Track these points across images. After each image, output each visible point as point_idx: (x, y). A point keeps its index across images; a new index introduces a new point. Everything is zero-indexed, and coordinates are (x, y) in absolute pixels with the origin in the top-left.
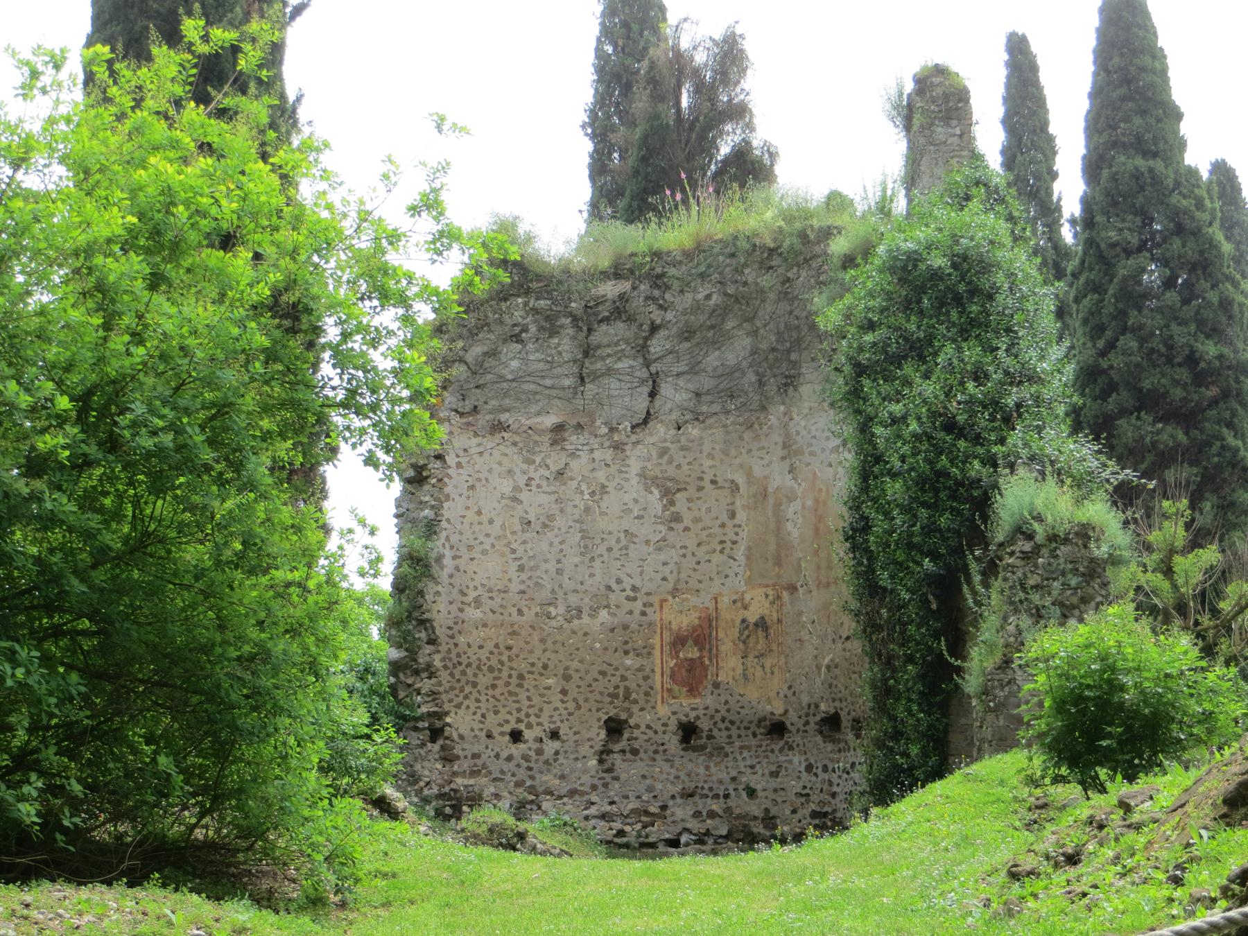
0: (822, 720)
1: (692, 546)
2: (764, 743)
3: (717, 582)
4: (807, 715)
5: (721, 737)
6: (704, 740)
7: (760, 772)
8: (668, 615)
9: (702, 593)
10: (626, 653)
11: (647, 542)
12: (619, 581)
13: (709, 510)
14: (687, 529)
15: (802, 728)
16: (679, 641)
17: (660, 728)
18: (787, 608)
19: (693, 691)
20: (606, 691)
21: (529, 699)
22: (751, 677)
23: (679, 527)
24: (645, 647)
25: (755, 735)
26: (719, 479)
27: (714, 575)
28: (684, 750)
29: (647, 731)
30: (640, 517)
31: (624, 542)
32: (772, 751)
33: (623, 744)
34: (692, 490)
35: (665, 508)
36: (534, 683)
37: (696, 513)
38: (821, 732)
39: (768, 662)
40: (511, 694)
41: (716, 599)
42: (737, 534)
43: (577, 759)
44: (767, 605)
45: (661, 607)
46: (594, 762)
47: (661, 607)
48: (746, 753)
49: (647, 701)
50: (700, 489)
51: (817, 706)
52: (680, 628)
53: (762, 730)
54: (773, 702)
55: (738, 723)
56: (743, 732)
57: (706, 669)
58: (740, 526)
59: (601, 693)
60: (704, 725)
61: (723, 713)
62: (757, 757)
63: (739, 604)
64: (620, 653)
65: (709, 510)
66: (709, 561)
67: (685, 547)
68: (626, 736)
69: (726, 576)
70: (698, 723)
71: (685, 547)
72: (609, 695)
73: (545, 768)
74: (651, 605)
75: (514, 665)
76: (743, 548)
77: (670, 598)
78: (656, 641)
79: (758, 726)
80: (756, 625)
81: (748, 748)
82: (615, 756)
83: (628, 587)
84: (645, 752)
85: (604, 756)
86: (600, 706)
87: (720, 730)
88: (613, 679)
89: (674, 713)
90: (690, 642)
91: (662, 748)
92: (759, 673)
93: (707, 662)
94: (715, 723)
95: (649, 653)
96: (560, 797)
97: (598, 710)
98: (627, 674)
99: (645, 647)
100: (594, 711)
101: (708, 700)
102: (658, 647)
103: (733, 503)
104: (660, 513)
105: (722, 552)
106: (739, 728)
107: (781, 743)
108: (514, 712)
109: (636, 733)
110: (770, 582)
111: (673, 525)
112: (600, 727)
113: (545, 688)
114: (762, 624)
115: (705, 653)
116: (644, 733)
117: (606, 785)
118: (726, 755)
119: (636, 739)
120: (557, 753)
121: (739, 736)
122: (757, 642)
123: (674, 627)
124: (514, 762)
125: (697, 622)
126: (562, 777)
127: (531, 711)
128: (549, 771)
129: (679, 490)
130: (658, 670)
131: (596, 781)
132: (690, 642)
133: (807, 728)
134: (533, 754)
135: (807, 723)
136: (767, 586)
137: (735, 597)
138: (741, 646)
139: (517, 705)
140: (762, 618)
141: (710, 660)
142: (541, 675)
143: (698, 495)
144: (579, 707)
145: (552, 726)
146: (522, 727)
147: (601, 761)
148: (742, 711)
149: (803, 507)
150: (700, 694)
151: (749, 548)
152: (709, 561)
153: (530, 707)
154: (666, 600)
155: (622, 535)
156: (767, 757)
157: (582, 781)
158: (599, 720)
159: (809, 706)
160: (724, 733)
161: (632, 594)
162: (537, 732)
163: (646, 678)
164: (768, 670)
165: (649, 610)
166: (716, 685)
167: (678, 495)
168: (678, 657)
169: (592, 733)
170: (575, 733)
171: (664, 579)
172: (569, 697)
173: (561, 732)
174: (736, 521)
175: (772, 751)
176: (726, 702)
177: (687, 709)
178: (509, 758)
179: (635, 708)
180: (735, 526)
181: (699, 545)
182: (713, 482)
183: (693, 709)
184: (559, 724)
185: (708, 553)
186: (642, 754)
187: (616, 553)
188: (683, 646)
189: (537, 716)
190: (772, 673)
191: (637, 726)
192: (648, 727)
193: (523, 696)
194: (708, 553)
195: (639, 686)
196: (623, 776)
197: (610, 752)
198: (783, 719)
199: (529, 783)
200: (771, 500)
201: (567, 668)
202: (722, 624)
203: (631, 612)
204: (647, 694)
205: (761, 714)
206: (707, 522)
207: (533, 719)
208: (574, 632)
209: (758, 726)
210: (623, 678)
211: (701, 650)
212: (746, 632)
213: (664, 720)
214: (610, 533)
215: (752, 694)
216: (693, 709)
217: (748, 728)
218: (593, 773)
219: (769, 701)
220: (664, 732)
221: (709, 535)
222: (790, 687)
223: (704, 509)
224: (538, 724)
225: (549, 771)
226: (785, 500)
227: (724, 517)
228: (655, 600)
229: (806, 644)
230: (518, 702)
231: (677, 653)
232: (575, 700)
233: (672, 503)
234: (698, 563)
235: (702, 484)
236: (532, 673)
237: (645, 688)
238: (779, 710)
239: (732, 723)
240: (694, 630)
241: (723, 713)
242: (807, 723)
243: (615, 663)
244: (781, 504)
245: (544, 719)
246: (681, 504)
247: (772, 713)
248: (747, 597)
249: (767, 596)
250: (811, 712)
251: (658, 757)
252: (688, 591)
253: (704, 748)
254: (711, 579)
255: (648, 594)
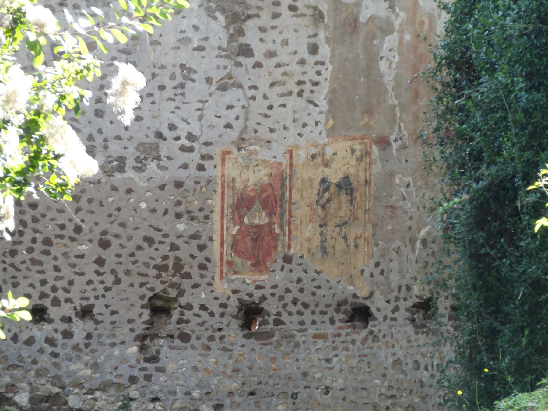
0: (414, 306)
1: (264, 87)
2: (344, 332)
3: (293, 131)
4: (397, 299)
5: (291, 322)
6: (271, 326)
7: (337, 367)
8: (232, 170)
9: (274, 145)
10: (178, 216)
11: (209, 80)
12: (172, 127)
13: (285, 43)
14: (258, 65)
15: (390, 315)
16: (243, 204)
17: (217, 310)
18: (377, 167)
19: (258, 265)
20: (153, 263)
21: (57, 269)
22: (330, 250)
23: (248, 62)
24: (201, 210)
25: (332, 322)
26: (298, 4)
27: (289, 123)
28: (245, 336)
29: (202, 313)
30: (200, 49)
31: (179, 79)
32: (353, 342)
33: (172, 326)
34: (265, 19)
35: (232, 38)
36: (64, 250)
37: (271, 47)
38: (413, 321)
39: (353, 232)
40: (34, 262)
41: (291, 152)
42: (319, 73)
43: (113, 345)
44: (353, 162)
45: (223, 160)
46: (135, 349)
47: (223, 160)
48: (320, 343)
49: (202, 276)
50: (276, 16)
51: (409, 288)
52: (246, 187)
53: (342, 316)
54: (357, 283)
55: (312, 307)
56: (318, 318)
57: (275, 238)
58: (323, 63)
59: (147, 265)
60: (271, 306)
61: (295, 293)
62: (334, 349)
63: (319, 160)
64: (170, 216)
65: (285, 43)
66: (284, 105)
67: (255, 88)
68: (175, 315)
69: (305, 125)
70: (264, 305)
71: (255, 88)
72: (155, 267)
73: (74, 354)
74: (211, 158)
75: (39, 226)
76: (325, 91)
77: (234, 150)
78: (216, 202)
79: (337, 311)
80: (339, 186)
81: (323, 337)
82: (162, 341)
83: (183, 134)
84: (198, 338)
85: (147, 342)
86: (145, 280)
87: (290, 314)
88: (160, 247)
89: (235, 292)
90: (257, 205)
91: (218, 334)
92: (340, 245)
93: (277, 231)
94: (285, 306)
95: (207, 217)
96: (91, 391)
97: (142, 285)
98: (179, 242)
99: (201, 210)
100: (137, 286)
101: (275, 277)
102: (218, 209)
103: (315, 35)
104: (225, 46)
105: (300, 94)
106: (313, 313)
107: (365, 332)
108: (38, 285)
109: (188, 314)
110: (358, 135)
111: (241, 59)
112: (143, 307)
113: (77, 257)
114: (346, 185)
115: (276, 219)
116: (197, 315)
117: (148, 378)
118: (297, 345)
119: (188, 322)
120: (89, 336)
121: (314, 322)
122: (340, 208)
123: (239, 185)
124: (36, 347)
125: (266, 180)
126: (95, 366)
127: (59, 284)
128: (79, 358)
129: (249, 17)
130: (217, 238)
131: (136, 373)
132: (257, 205)
133: (396, 315)
134: (59, 336)
135: (396, 309)
136: (354, 139)
137: (313, 151)
138: (320, 210)
139: (42, 277)
140: (347, 178)
141: (281, 227)
142: (73, 239)
143: (275, 22)
144: (118, 281)
145: (85, 303)
146: (47, 303)
147: (143, 348)
148: (319, 292)
149: (401, 44)
150: (267, 269)
151: (333, 91)
152: (284, 105)
153: (57, 279)
154: (229, 153)
155: (178, 71)
156: (347, 349)
157: (119, 372)
158: (142, 297)
159: (400, 288)
160: (296, 318)
161: (187, 143)
162: (66, 310)
163: (202, 248)
164: (351, 242)
165: (207, 164)
166: (288, 259)
167: (249, 23)
168: (242, 222)
169: (133, 314)
170: (113, 313)
171: (228, 126)
172: (106, 268)
173: (95, 311)
174: (318, 58)
175: (353, 342)
176: (299, 280)
177: (251, 288)
178: (30, 341)
179: (186, 284)
180: (316, 63)
181: (272, 85)
182: (292, 8)
183: (258, 287)
184: (92, 301)
185: (283, 95)
186: (193, 341)
187: (169, 92)
188: (249, 208)
189: (67, 291)
190: (356, 246)
191: (189, 307)
192: (203, 307)
193: (48, 265)
194: (283, 95)
195: (192, 257)
196: (171, 367)
197: (155, 336)
198: (368, 303)
199: (53, 371)
200: (362, 33)
201: (104, 233)
202: (298, 184)
203: (185, 166)
204: (202, 267)
205: (340, 297)
206: (283, 57)
207: (61, 295)
208: (114, 189)
209: (337, 311)
210: (174, 247)
211: (270, 215)
212: (327, 195)
213: (223, 300)
214: (163, 67)
215: (330, 271)
216: (258, 287)
217: (325, 313)
218: (133, 362)
219: (351, 280)
220: (222, 315)
221: (285, 74)
222: (377, 264)
223: (279, 41)
224: (68, 300)
225: (79, 358)
226: (379, 34)
227: (304, 53)
228: (216, 151)
229: (399, 212)
230: (42, 272)
231: (241, 217)
232: (113, 272)
233: (241, 32)
234: (271, 107)
235: (277, 10)
236: (62, 237)
237: (201, 257)
238: (363, 293)
239: (306, 305)
240: (263, 190)
241: (295, 293)
242: (396, 309)
243: (166, 229)
244: (374, 38)
245: (75, 295)
246: (251, 37)
247: (355, 296)
248: (329, 151)
249: (353, 151)
250: (402, 295)
251: (213, 345)
252: (258, 141)
253: (270, 335)
254: (285, 128)
255: (207, 144)
